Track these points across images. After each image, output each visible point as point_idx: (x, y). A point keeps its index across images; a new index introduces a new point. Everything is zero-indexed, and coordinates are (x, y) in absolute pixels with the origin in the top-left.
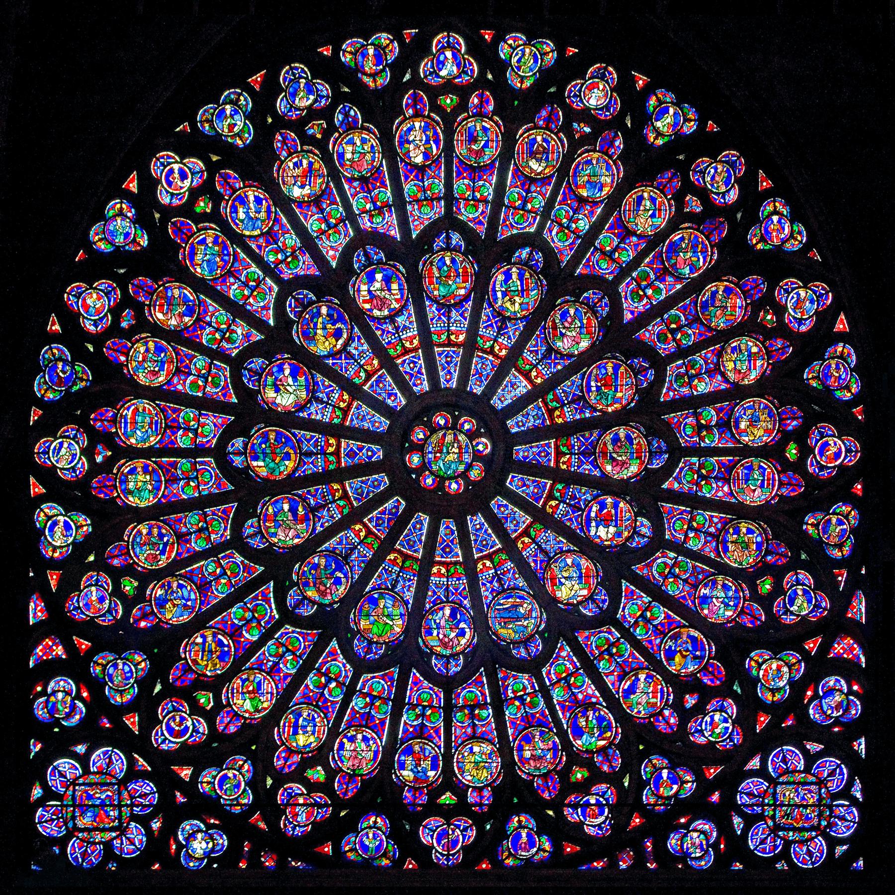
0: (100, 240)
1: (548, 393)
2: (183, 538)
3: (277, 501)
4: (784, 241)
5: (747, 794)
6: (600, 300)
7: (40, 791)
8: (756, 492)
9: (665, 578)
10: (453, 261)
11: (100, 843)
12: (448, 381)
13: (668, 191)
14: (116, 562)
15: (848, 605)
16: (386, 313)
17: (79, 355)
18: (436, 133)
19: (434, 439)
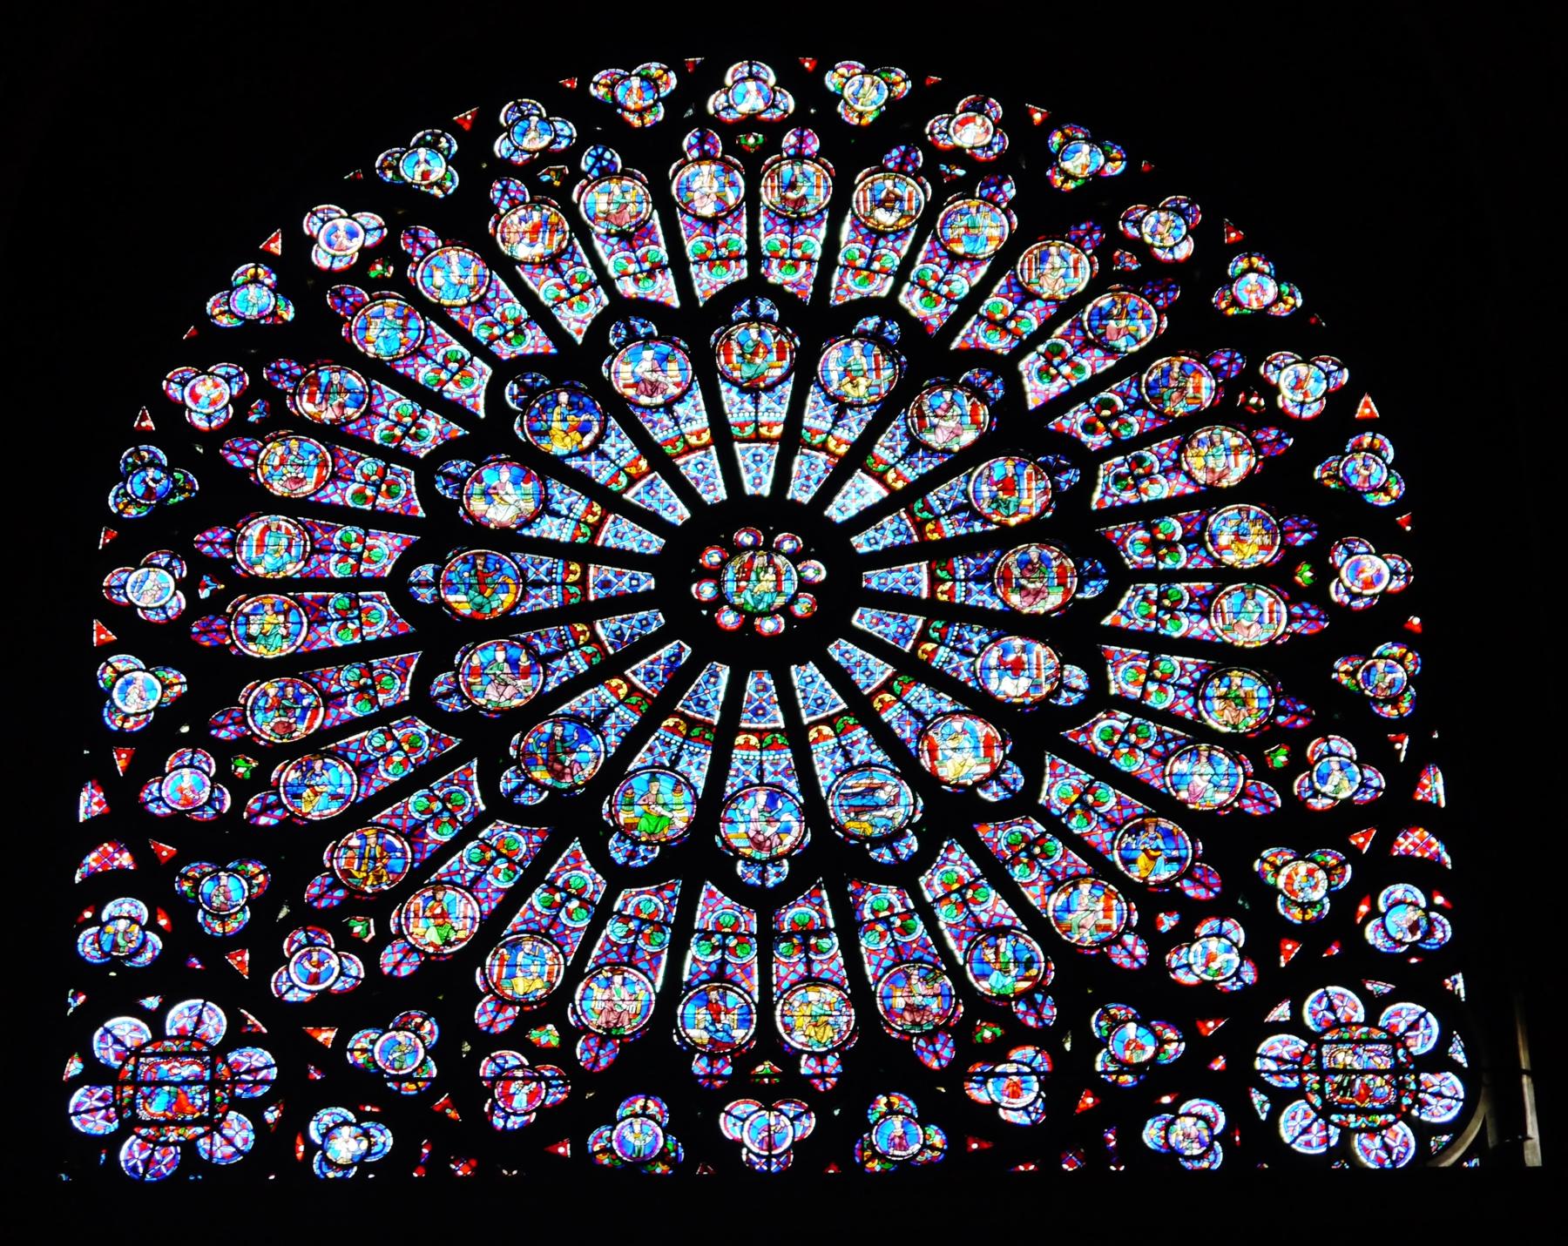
0: (223, 313)
2: (332, 700)
4: (1268, 307)
6: (991, 381)
7: (81, 1066)
8: (1253, 630)
9: (1115, 747)
10: (761, 333)
11: (175, 1144)
13: (1088, 245)
15: (1415, 783)
16: (659, 399)
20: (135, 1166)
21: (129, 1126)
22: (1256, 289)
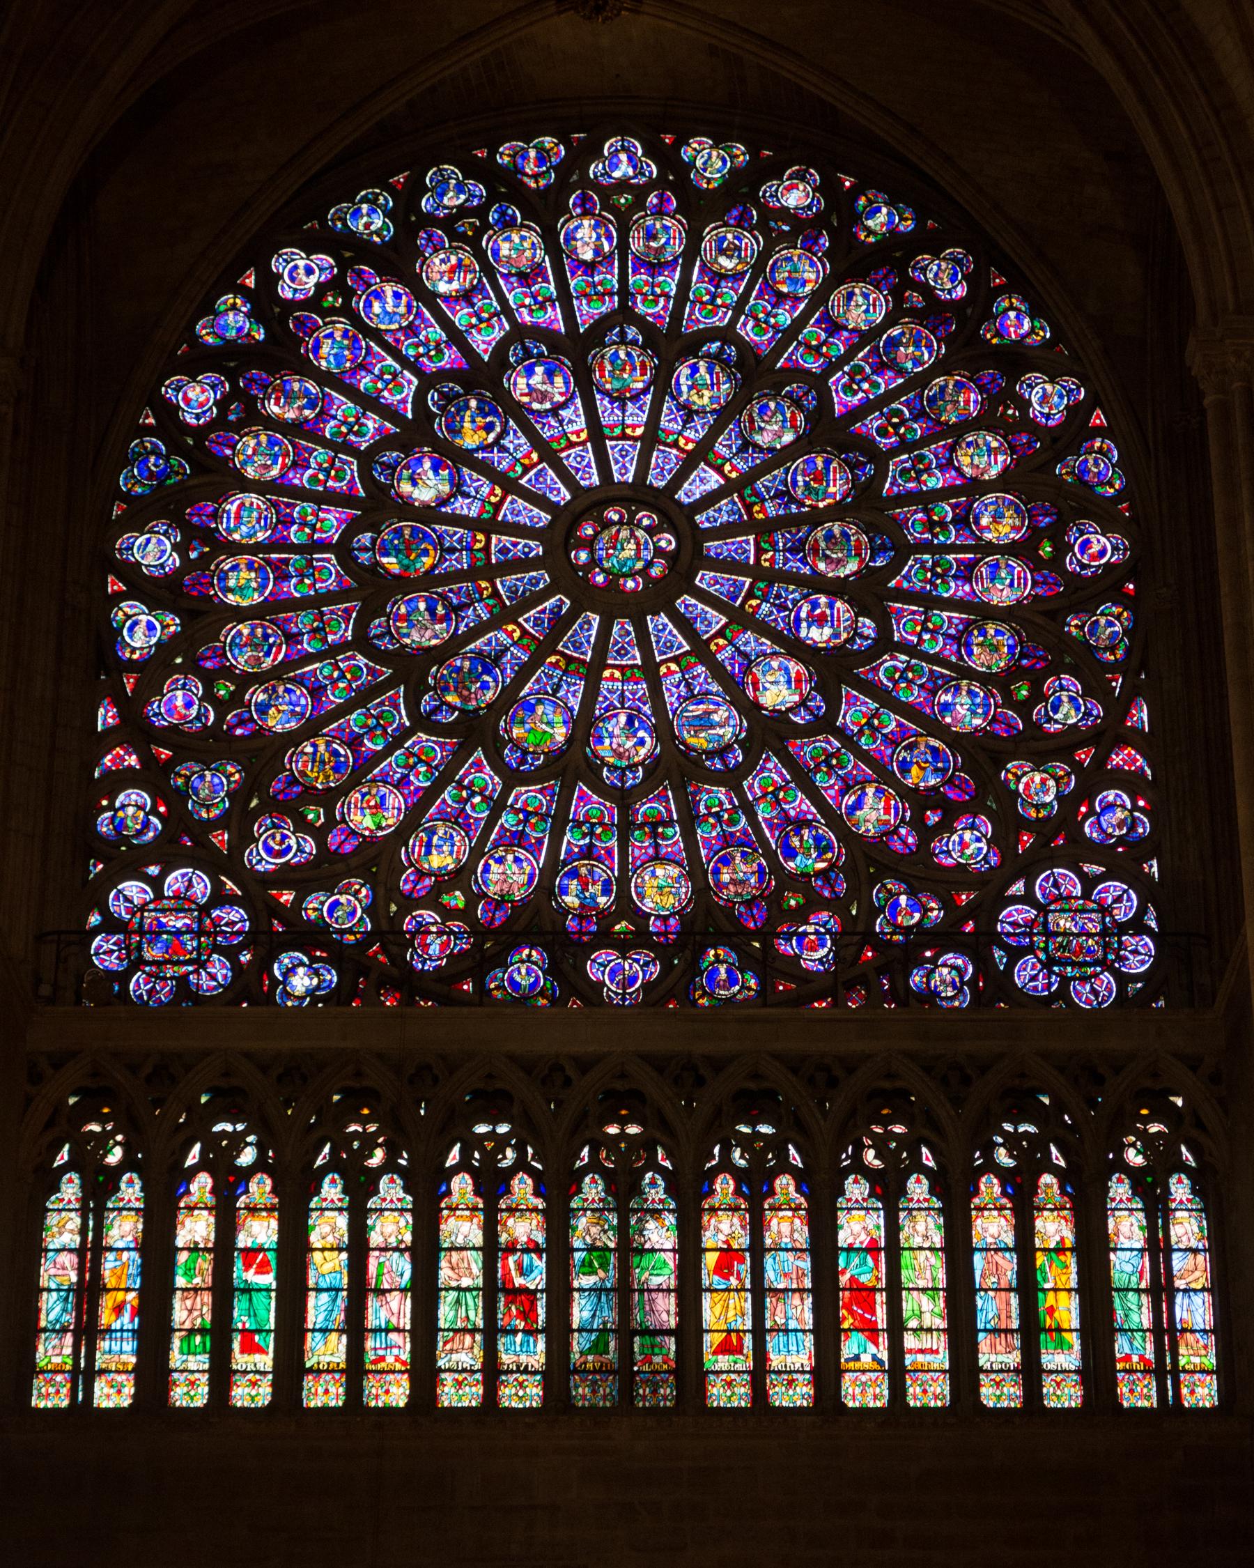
0: (208, 334)
1: (744, 488)
2: (292, 639)
3: (411, 600)
5: (1010, 924)
6: (806, 394)
9: (896, 683)
10: (628, 354)
11: (172, 978)
12: (622, 475)
14: (209, 664)
15: (1126, 713)
16: (548, 405)
17: (176, 448)
18: (608, 231)
19: (606, 536)
20: (141, 995)
21: (138, 964)
22: (1018, 323)
